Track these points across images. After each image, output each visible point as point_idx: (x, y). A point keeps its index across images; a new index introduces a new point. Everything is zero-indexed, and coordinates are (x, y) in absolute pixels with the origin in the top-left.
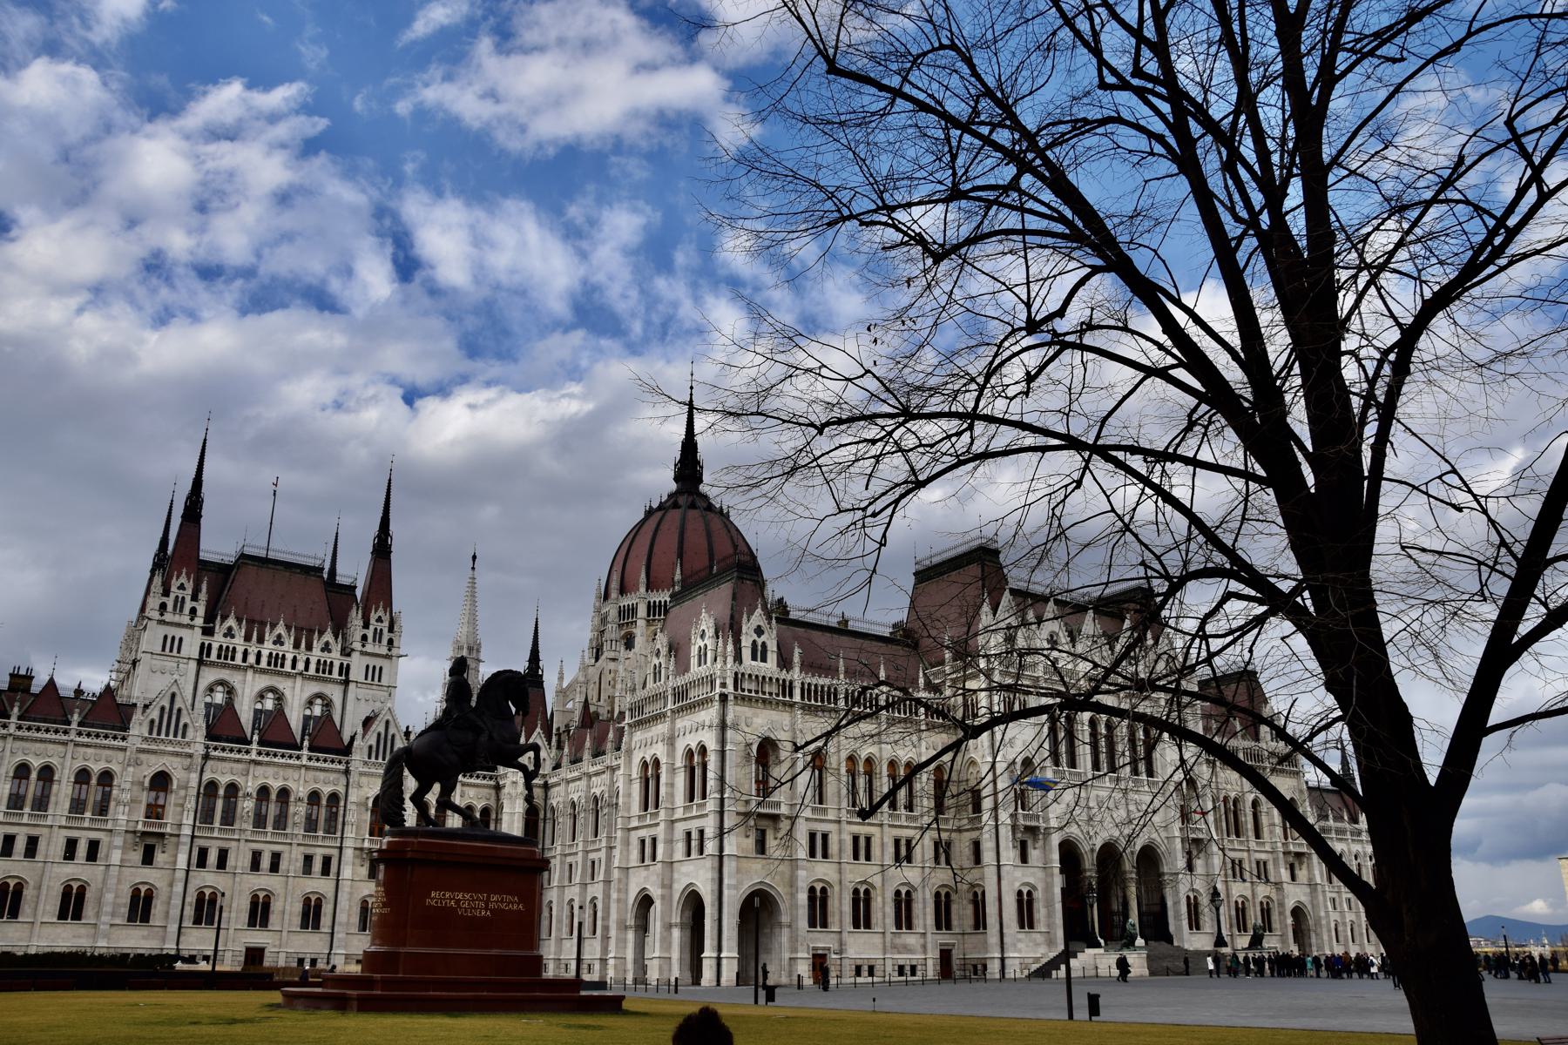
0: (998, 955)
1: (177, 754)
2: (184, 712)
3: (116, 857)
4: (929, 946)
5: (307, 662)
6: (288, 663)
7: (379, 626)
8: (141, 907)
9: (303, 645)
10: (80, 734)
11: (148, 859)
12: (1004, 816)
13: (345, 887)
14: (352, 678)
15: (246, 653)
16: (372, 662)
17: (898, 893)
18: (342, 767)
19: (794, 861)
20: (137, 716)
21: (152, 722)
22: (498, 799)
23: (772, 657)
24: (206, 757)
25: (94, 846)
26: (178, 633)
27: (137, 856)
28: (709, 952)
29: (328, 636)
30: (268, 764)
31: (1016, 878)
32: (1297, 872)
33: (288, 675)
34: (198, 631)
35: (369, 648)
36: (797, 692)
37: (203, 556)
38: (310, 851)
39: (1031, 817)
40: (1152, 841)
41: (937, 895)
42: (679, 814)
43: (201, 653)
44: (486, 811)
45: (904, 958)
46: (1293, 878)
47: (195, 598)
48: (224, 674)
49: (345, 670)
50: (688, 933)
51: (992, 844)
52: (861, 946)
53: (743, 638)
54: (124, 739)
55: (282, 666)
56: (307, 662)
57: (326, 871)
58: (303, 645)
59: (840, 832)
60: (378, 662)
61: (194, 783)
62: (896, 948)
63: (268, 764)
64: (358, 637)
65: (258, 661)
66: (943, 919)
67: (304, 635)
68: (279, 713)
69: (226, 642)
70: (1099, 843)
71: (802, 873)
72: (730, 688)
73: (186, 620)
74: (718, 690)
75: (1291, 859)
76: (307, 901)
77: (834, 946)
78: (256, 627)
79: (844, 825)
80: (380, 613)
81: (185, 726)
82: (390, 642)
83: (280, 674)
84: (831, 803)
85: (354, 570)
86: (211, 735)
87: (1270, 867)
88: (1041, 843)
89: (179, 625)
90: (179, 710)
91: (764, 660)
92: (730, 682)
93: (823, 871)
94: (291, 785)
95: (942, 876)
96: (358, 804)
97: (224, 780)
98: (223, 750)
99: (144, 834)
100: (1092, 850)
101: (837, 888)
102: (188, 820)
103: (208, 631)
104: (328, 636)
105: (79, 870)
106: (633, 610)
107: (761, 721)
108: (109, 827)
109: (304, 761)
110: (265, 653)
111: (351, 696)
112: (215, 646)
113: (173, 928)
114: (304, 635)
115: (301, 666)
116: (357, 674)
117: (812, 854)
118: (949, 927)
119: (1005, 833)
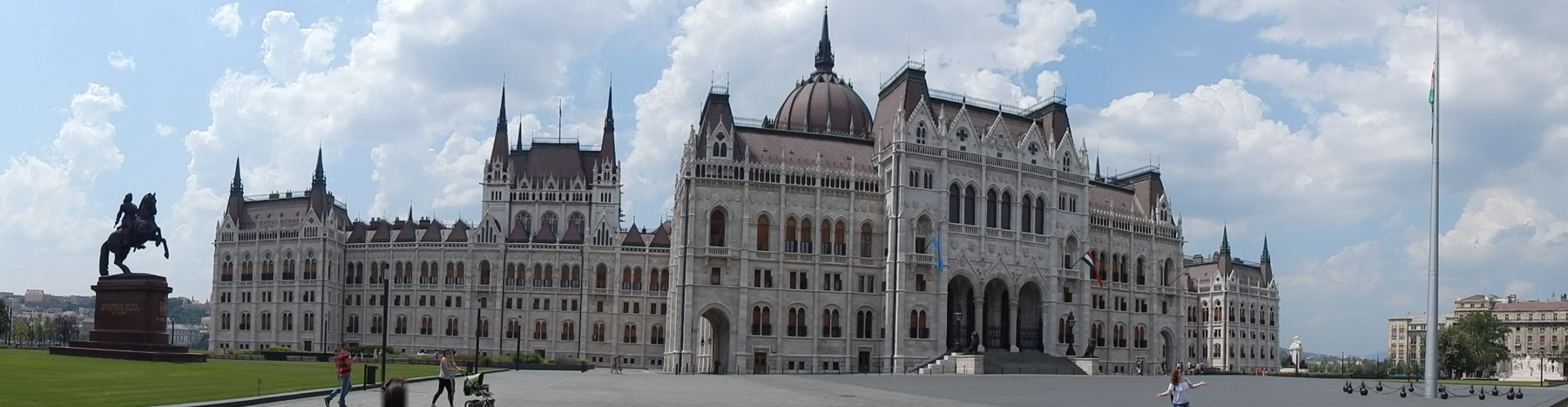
16: (604, 191)
23: (730, 153)
41: (860, 313)
45: (826, 356)
60: (608, 191)
71: (744, 298)
72: (693, 175)
91: (724, 154)
104: (578, 180)
107: (715, 196)
116: (596, 198)
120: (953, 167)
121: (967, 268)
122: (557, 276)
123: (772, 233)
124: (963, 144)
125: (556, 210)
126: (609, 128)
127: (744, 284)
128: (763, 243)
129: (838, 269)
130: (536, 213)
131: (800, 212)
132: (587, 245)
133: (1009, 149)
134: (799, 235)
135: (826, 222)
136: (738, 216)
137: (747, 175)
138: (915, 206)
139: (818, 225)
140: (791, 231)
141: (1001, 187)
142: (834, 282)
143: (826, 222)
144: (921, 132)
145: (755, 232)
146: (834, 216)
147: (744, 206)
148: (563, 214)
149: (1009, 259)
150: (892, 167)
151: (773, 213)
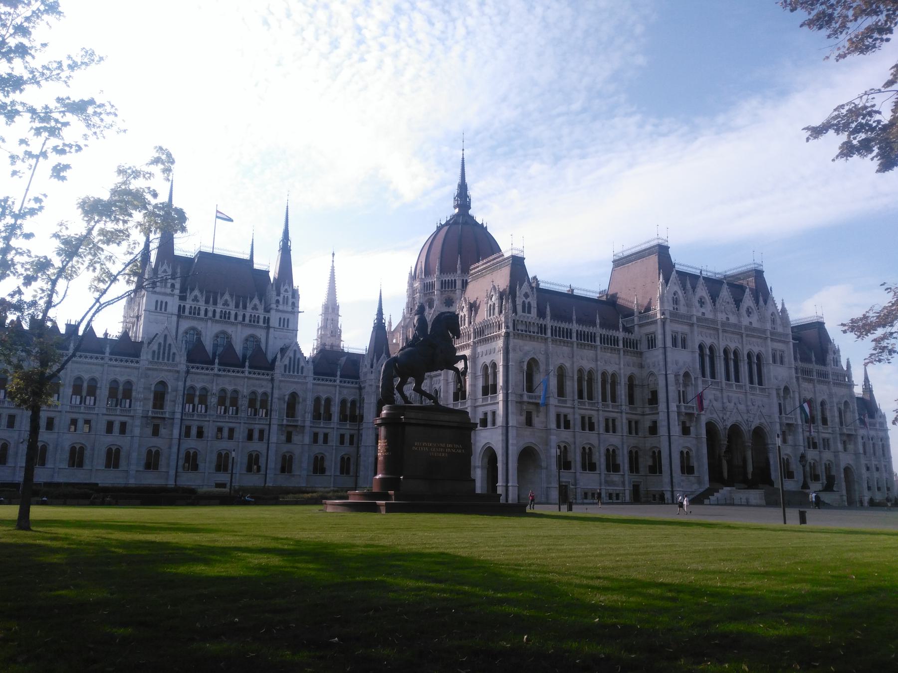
0: (669, 489)
1: (170, 371)
2: (173, 346)
3: (137, 431)
4: (627, 483)
5: (244, 316)
6: (232, 317)
8: (152, 461)
9: (241, 306)
10: (111, 360)
11: (156, 432)
12: (673, 407)
13: (273, 447)
14: (271, 324)
15: (206, 311)
16: (283, 316)
17: (608, 450)
18: (269, 377)
19: (547, 430)
20: (144, 349)
21: (154, 352)
22: (360, 395)
23: (534, 311)
24: (188, 372)
25: (123, 425)
27: (149, 431)
28: (500, 483)
29: (256, 301)
30: (225, 376)
31: (680, 443)
32: (848, 446)
33: (232, 324)
34: (177, 298)
35: (281, 307)
36: (549, 331)
37: (177, 253)
38: (252, 427)
39: (690, 407)
40: (761, 424)
41: (630, 452)
42: (480, 402)
43: (179, 311)
44: (353, 403)
45: (611, 489)
46: (845, 450)
49: (267, 321)
50: (486, 472)
51: (665, 423)
52: (588, 481)
53: (517, 299)
54: (137, 362)
55: (229, 318)
56: (244, 316)
57: (261, 439)
58: (241, 306)
59: (574, 414)
61: (181, 388)
62: (607, 483)
63: (225, 376)
64: (274, 301)
65: (214, 315)
66: (634, 466)
68: (230, 347)
70: (729, 424)
71: (553, 438)
73: (169, 291)
74: (504, 330)
75: (845, 438)
76: (250, 456)
77: (571, 480)
79: (576, 410)
80: (286, 287)
81: (174, 354)
83: (226, 323)
84: (569, 397)
85: (267, 262)
86: (190, 360)
87: (831, 442)
89: (165, 294)
90: (170, 345)
91: (529, 312)
92: (511, 325)
93: (565, 435)
94: (239, 388)
95: (633, 441)
96: (279, 399)
97: (199, 385)
98: (198, 368)
99: (153, 418)
100: (725, 428)
101: (573, 446)
102: (178, 409)
104: (256, 301)
105: (115, 439)
106: (432, 285)
107: (530, 348)
108: (132, 414)
109: (247, 374)
110: (218, 311)
111: (271, 336)
112: (188, 307)
113: (172, 472)
114: (242, 300)
115: (240, 318)
116: (274, 322)
117: (558, 426)
118: (637, 471)
119: (674, 416)
121: (715, 416)
124: (703, 310)
128: (561, 392)
131: (587, 365)
135: (604, 374)
142: (611, 426)
146: (610, 369)
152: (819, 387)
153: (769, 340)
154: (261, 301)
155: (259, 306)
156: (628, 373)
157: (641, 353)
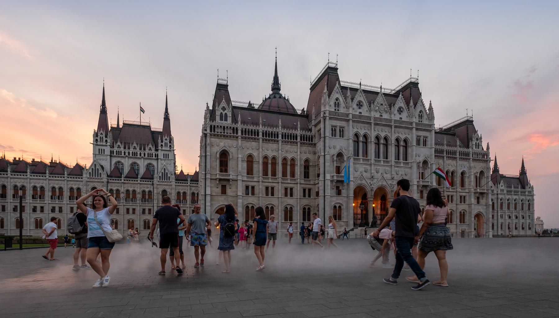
7: (166, 141)
26: (103, 148)
33: (139, 158)
35: (164, 148)
47: (106, 137)
48: (119, 159)
49: (157, 156)
60: (167, 153)
63: (128, 183)
67: (143, 146)
69: (118, 150)
72: (208, 131)
78: (127, 145)
82: (170, 146)
88: (346, 187)
91: (226, 120)
103: (112, 147)
104: (150, 146)
107: (221, 144)
110: (131, 152)
112: (115, 151)
116: (161, 156)
120: (355, 124)
122: (139, 196)
123: (255, 166)
125: (138, 161)
126: (167, 119)
127: (240, 193)
128: (250, 171)
129: (292, 185)
130: (127, 163)
131: (270, 154)
132: (156, 181)
133: (386, 112)
134: (270, 165)
135: (285, 159)
136: (235, 156)
137: (240, 132)
138: (334, 147)
139: (280, 162)
140: (265, 164)
141: (383, 135)
143: (285, 159)
144: (337, 105)
145: (245, 165)
147: (239, 150)
148: (142, 165)
149: (388, 176)
150: (322, 125)
151: (255, 154)
152: (460, 163)
153: (414, 129)
154: (153, 146)
155: (152, 148)
156: (304, 158)
157: (315, 144)
